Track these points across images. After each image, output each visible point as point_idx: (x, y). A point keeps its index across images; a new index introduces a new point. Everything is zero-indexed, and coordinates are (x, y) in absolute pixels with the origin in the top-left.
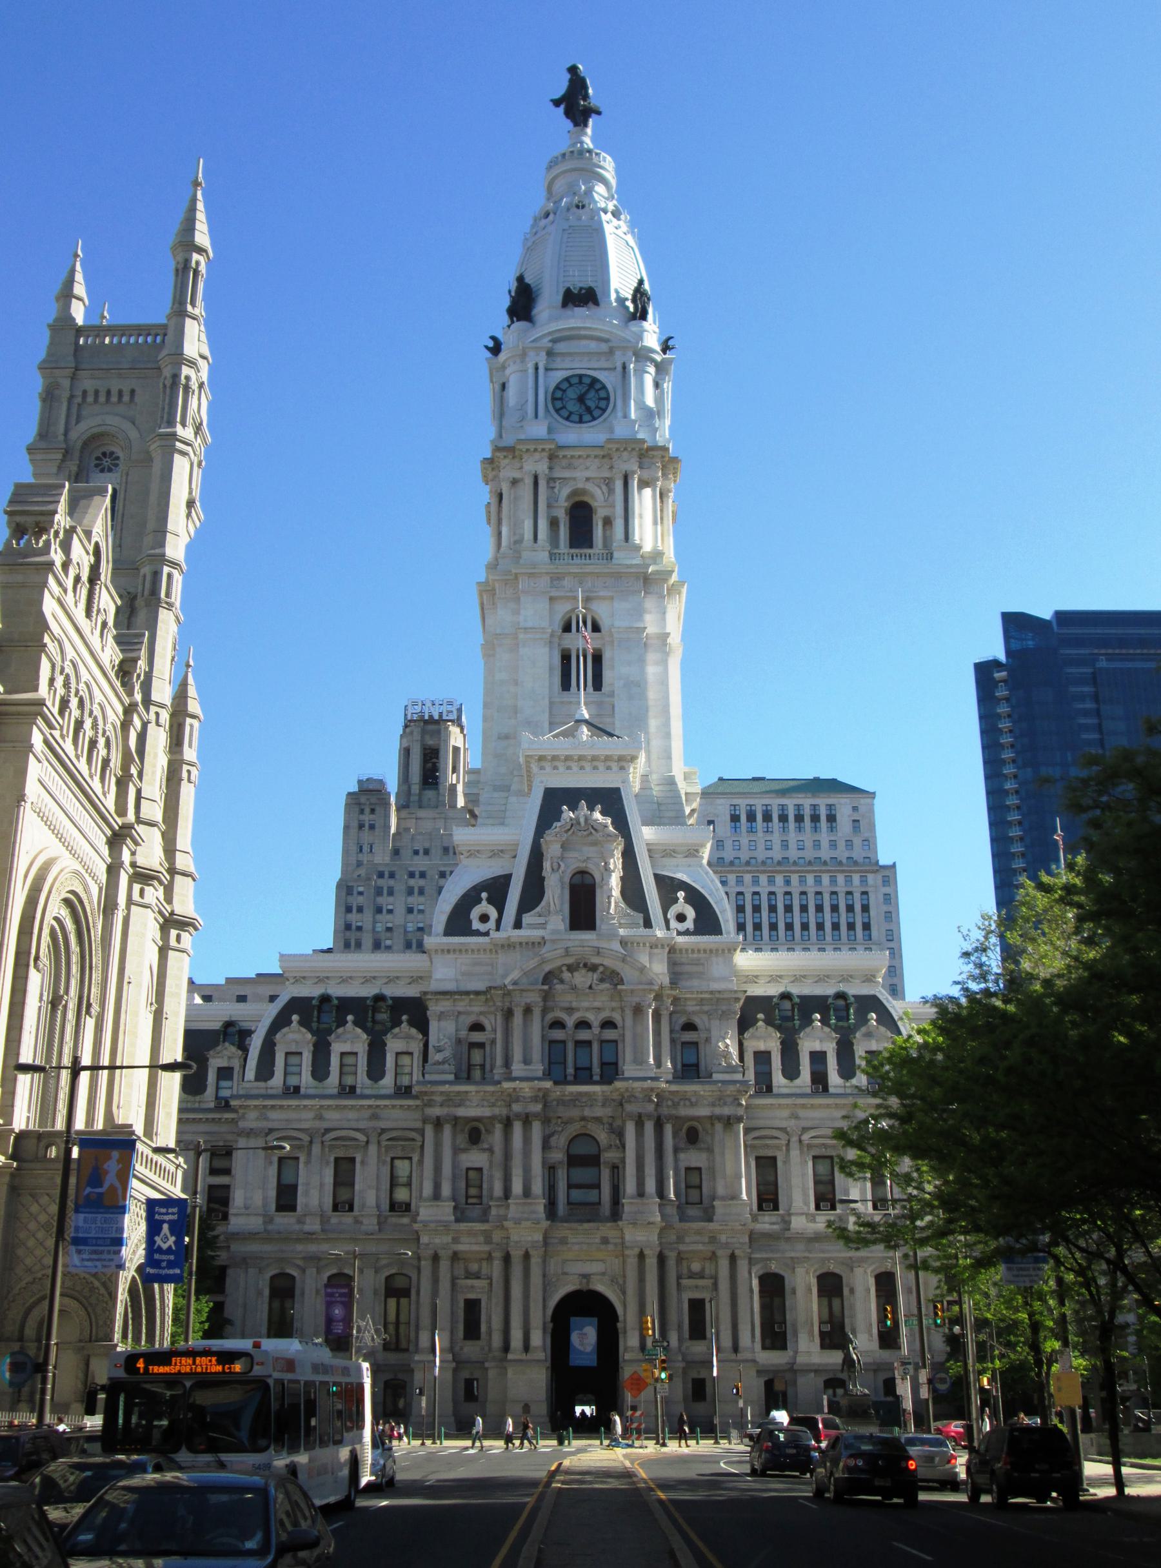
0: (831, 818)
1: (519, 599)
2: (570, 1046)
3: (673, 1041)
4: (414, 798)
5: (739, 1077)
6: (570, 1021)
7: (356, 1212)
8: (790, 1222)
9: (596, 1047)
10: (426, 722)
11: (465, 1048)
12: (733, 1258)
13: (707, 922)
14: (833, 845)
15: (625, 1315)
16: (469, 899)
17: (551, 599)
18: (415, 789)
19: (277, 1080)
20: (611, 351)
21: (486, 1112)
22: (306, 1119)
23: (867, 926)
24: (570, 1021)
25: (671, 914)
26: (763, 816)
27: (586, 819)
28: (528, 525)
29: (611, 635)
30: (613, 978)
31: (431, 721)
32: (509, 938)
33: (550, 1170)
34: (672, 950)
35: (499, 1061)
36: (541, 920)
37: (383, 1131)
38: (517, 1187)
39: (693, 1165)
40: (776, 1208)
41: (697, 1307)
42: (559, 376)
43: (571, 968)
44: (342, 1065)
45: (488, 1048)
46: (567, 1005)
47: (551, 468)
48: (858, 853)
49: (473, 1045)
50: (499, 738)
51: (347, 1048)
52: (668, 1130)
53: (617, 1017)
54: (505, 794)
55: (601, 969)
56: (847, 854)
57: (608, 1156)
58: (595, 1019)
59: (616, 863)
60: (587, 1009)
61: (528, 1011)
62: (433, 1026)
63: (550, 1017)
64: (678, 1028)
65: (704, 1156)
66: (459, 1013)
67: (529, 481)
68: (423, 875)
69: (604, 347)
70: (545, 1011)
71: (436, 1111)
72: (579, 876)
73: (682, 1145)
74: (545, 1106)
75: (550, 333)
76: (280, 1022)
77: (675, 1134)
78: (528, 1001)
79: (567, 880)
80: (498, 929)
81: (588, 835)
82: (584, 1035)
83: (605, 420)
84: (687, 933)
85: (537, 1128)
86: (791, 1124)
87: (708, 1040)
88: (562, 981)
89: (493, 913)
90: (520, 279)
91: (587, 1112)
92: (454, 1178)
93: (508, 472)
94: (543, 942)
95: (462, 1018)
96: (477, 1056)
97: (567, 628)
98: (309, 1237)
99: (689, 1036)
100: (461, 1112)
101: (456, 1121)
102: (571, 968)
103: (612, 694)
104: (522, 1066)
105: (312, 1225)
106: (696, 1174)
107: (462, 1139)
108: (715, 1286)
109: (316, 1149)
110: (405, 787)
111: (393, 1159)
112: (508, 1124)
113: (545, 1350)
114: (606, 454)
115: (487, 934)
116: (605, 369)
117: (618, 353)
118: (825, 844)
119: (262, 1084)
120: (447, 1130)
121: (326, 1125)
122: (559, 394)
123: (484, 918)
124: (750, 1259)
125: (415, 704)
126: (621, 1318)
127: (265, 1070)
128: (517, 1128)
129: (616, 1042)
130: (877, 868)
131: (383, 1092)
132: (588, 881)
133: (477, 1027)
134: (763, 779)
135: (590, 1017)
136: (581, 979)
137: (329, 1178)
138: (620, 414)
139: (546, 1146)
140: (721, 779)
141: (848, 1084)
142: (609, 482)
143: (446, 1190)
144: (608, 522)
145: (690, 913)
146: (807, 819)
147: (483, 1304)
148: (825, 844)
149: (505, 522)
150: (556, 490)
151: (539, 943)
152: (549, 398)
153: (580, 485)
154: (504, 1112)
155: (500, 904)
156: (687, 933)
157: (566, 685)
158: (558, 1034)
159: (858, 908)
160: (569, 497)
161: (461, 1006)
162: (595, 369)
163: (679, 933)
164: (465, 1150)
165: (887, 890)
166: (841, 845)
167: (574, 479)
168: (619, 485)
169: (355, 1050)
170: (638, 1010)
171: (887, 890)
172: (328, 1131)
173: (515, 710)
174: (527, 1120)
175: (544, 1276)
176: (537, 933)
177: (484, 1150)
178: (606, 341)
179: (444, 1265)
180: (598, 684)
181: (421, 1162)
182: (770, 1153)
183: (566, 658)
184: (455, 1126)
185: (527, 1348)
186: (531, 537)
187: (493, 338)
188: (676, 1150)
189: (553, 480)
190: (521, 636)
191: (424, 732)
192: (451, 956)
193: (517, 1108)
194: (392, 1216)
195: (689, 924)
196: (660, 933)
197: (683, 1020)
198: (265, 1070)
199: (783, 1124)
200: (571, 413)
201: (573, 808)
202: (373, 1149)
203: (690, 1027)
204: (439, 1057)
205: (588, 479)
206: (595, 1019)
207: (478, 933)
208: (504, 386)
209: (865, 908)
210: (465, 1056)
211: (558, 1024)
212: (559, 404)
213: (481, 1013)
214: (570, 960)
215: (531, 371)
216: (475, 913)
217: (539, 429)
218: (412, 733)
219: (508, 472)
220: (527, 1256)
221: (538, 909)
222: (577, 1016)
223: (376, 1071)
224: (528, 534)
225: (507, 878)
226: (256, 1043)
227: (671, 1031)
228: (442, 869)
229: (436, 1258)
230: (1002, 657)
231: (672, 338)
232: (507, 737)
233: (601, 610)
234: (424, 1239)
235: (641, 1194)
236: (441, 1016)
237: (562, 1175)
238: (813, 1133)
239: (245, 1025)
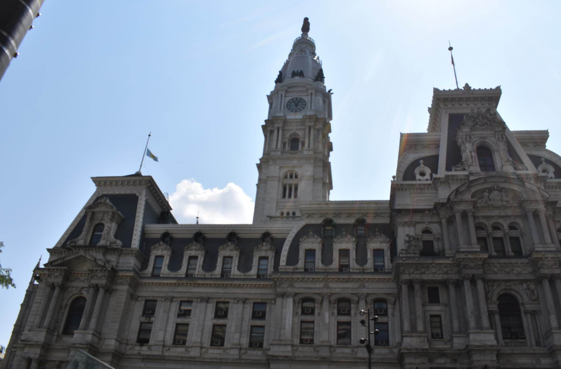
38: (472, 324)
51: (344, 246)
53: (519, 221)
66: (417, 223)
82: (499, 234)
85: (480, 285)
95: (418, 226)
100: (425, 277)
101: (423, 283)
112: (458, 285)
119: (292, 267)
128: (467, 284)
135: (501, 221)
143: (420, 328)
161: (417, 218)
174: (473, 281)
213: (430, 222)
234: (407, 360)
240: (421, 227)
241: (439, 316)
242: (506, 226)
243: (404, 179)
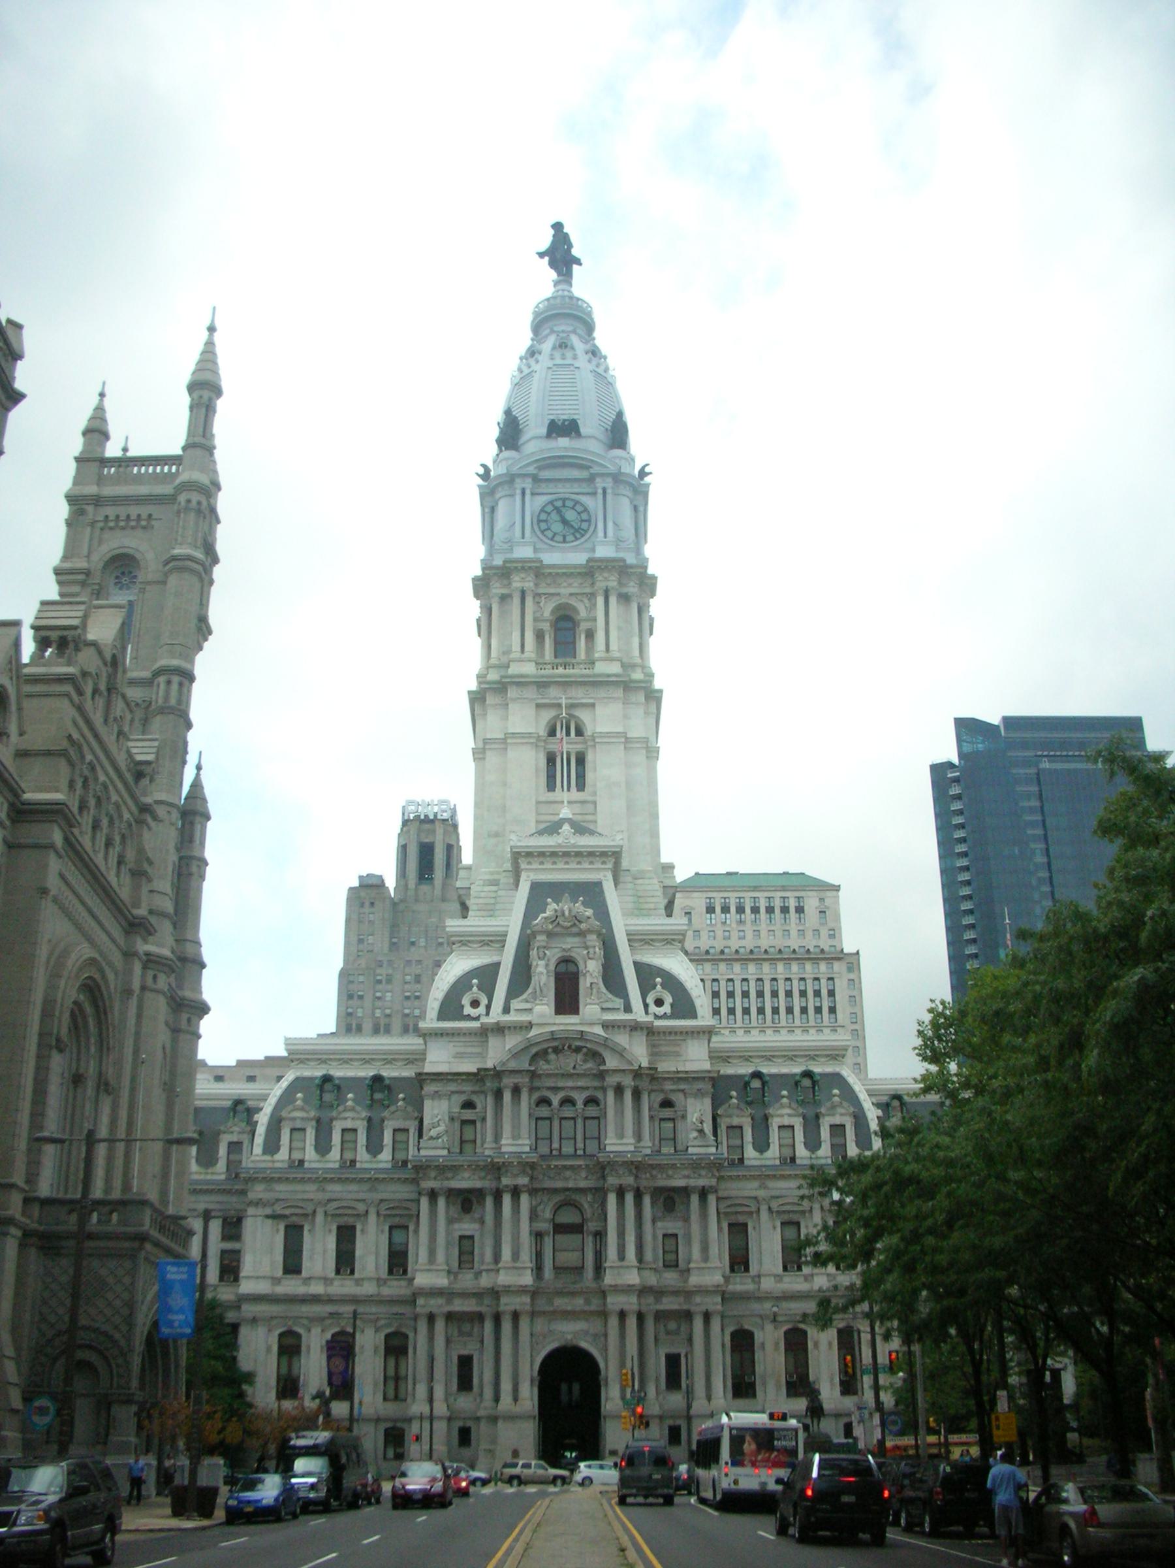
0: (800, 910)
1: (507, 705)
2: (556, 1123)
3: (651, 1118)
4: (411, 893)
5: (713, 1150)
6: (555, 1101)
7: (357, 1275)
8: (760, 1282)
9: (580, 1121)
10: (422, 822)
11: (457, 1125)
12: (707, 1316)
13: (684, 1006)
14: (801, 932)
15: (607, 1368)
16: (461, 986)
17: (538, 706)
18: (412, 882)
19: (283, 1155)
20: (591, 479)
21: (478, 1184)
22: (310, 1191)
23: (833, 1010)
24: (556, 1100)
25: (650, 1000)
26: (737, 908)
27: (570, 911)
28: (516, 636)
29: (593, 738)
30: (595, 1055)
31: (427, 821)
32: (498, 1023)
33: (538, 1236)
34: (650, 1031)
35: (489, 1137)
36: (528, 1006)
37: (382, 1201)
38: (506, 1253)
39: (670, 1232)
40: (747, 1269)
41: (673, 1362)
42: (541, 500)
43: (556, 1050)
44: (342, 1142)
45: (478, 1125)
46: (553, 1085)
47: (536, 585)
48: (825, 943)
49: (464, 1122)
50: (489, 836)
51: (349, 1124)
52: (647, 1200)
53: (599, 1095)
54: (494, 888)
55: (585, 1050)
56: (814, 943)
57: (592, 1226)
58: (580, 1098)
59: (599, 952)
60: (572, 1088)
61: (516, 1091)
62: (428, 1104)
63: (536, 1095)
64: (656, 1105)
65: (680, 1224)
66: (453, 1092)
67: (516, 600)
68: (419, 962)
69: (584, 474)
70: (532, 1089)
71: (428, 1184)
72: (563, 965)
73: (660, 1214)
74: (532, 1178)
75: (537, 461)
76: (287, 1098)
77: (653, 1204)
78: (516, 1081)
79: (552, 967)
80: (488, 1014)
81: (571, 926)
83: (586, 541)
84: (664, 1016)
85: (524, 1199)
86: (761, 1193)
87: (684, 1117)
88: (548, 1062)
89: (484, 1001)
90: (508, 413)
91: (571, 1185)
92: (448, 1244)
93: (497, 589)
94: (530, 1025)
96: (468, 1130)
97: (552, 733)
98: (315, 1299)
99: (667, 1113)
102: (556, 1050)
103: (594, 794)
104: (510, 1142)
105: (317, 1289)
106: (673, 1241)
107: (455, 1210)
108: (690, 1340)
109: (320, 1218)
110: (402, 883)
111: (391, 1228)
112: (498, 1196)
113: (532, 1400)
114: (590, 570)
115: (477, 1018)
116: (588, 494)
117: (598, 480)
118: (794, 933)
119: (268, 1158)
120: (441, 1202)
121: (328, 1196)
122: (543, 516)
123: (475, 1004)
124: (722, 1317)
125: (410, 802)
126: (603, 1372)
127: (271, 1146)
128: (507, 1200)
129: (598, 1118)
130: (840, 956)
131: (381, 1166)
132: (572, 968)
133: (469, 1105)
134: (737, 873)
135: (575, 1095)
136: (569, 1062)
137: (331, 1243)
138: (601, 533)
139: (534, 1216)
140: (697, 874)
141: (813, 1156)
142: (592, 596)
144: (590, 635)
145: (668, 1000)
146: (777, 910)
147: (475, 1359)
148: (794, 933)
149: (494, 633)
150: (542, 604)
151: (526, 1027)
152: (535, 521)
153: (563, 600)
154: (494, 1185)
155: (489, 989)
156: (664, 1016)
157: (551, 786)
158: (544, 1111)
159: (824, 992)
160: (553, 612)
161: (453, 1087)
162: (577, 494)
164: (459, 1220)
165: (852, 976)
166: (809, 934)
167: (558, 594)
168: (600, 601)
169: (355, 1127)
170: (619, 1090)
171: (852, 976)
172: (329, 1201)
173: (504, 809)
174: (516, 1192)
175: (532, 1335)
176: (525, 1018)
177: (474, 1221)
178: (588, 468)
179: (440, 1325)
180: (581, 786)
181: (416, 1231)
182: (741, 1219)
183: (551, 760)
184: (448, 1198)
185: (516, 1399)
186: (519, 649)
187: (483, 466)
188: (654, 1221)
189: (539, 595)
190: (509, 741)
191: (419, 831)
192: (446, 1039)
193: (506, 1181)
194: (391, 1280)
195: (666, 1008)
196: (638, 1014)
197: (660, 1098)
198: (271, 1146)
199: (753, 1193)
200: (555, 534)
201: (557, 901)
202: (372, 1217)
203: (667, 1104)
204: (433, 1133)
205: (571, 594)
206: (580, 1098)
207: (469, 1018)
208: (493, 510)
209: (831, 993)
210: (458, 1133)
211: (544, 1101)
212: (543, 526)
213: (473, 1092)
214: (555, 1044)
215: (518, 498)
216: (466, 1001)
217: (524, 552)
218: (408, 831)
219: (497, 589)
220: (516, 1316)
221: (524, 996)
222: (561, 1095)
223: (374, 1147)
224: (516, 647)
225: (497, 965)
226: (263, 1119)
227: (650, 1109)
228: (438, 958)
229: (431, 1318)
230: (956, 761)
231: (647, 465)
232: (497, 835)
233: (584, 716)
234: (420, 1301)
235: (622, 1256)
236: (436, 1095)
237: (548, 1242)
238: (781, 1201)
239: (250, 1103)
240: (459, 1099)
241: (471, 1237)
242: (580, 1104)
243: (439, 1019)
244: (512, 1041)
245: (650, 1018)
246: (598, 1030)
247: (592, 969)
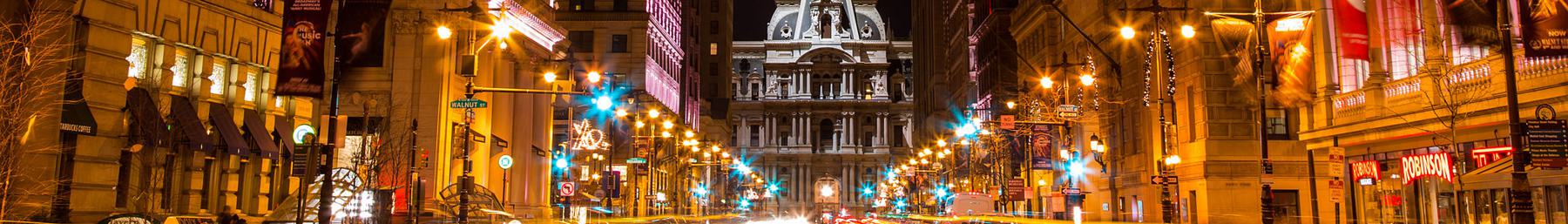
24: (822, 75)
53: (839, 73)
84: (868, 38)
94: (810, 45)
123: (786, 31)
139: (811, 124)
145: (870, 31)
156: (868, 38)
163: (865, 38)
176: (808, 41)
182: (899, 124)
188: (862, 125)
195: (869, 34)
196: (856, 40)
222: (824, 73)
225: (797, 14)
244: (804, 52)
245: (861, 41)
246: (840, 48)
247: (836, 19)
